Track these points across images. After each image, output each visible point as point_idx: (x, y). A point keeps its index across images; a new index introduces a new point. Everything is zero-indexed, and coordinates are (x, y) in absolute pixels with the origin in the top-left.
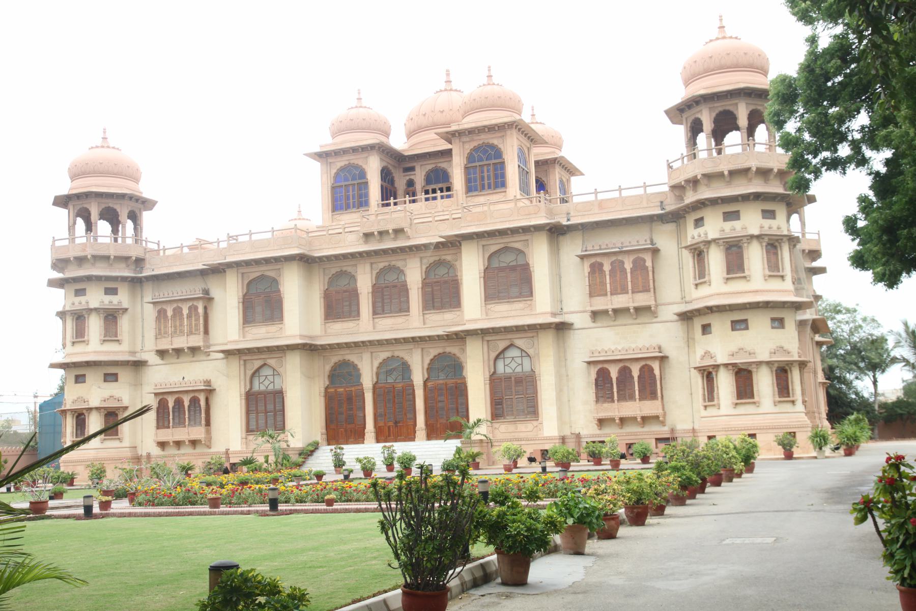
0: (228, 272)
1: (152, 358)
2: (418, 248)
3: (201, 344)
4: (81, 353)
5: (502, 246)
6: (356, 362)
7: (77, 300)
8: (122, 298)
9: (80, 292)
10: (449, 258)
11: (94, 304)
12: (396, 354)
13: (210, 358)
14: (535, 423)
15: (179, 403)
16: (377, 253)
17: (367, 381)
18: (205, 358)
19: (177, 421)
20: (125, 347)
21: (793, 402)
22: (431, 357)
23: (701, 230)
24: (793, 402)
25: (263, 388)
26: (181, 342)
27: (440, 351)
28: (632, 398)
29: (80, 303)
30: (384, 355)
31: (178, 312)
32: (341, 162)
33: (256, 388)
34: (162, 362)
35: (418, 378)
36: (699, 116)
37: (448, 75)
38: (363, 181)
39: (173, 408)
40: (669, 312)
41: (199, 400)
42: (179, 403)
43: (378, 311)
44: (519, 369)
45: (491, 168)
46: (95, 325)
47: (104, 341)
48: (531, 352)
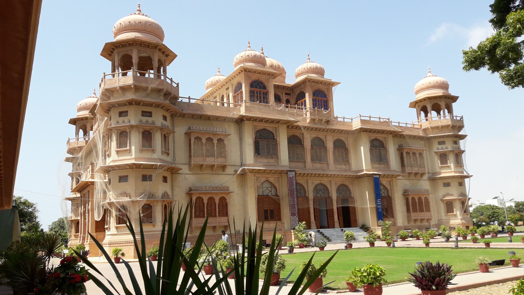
0: (246, 122)
1: (185, 169)
2: (334, 131)
3: (226, 164)
4: (128, 159)
5: (374, 138)
6: (304, 185)
7: (144, 119)
8: (168, 123)
9: (145, 114)
10: (343, 139)
11: (133, 123)
12: (322, 182)
13: (224, 173)
14: (392, 219)
15: (211, 199)
16: (316, 129)
17: (311, 196)
18: (221, 172)
19: (197, 213)
20: (169, 159)
21: (467, 214)
22: (338, 185)
23: (444, 146)
24: (467, 214)
25: (265, 194)
26: (210, 161)
27: (341, 183)
28: (423, 211)
29: (147, 122)
30: (317, 182)
31: (210, 140)
32: (255, 77)
33: (261, 194)
34: (190, 172)
35: (334, 196)
36: (439, 102)
37: (262, 50)
38: (253, 89)
39: (207, 203)
40: (425, 177)
41: (225, 199)
42: (211, 199)
43: (312, 160)
44: (383, 195)
45: (323, 102)
46: (158, 139)
47: (165, 152)
48: (388, 187)
